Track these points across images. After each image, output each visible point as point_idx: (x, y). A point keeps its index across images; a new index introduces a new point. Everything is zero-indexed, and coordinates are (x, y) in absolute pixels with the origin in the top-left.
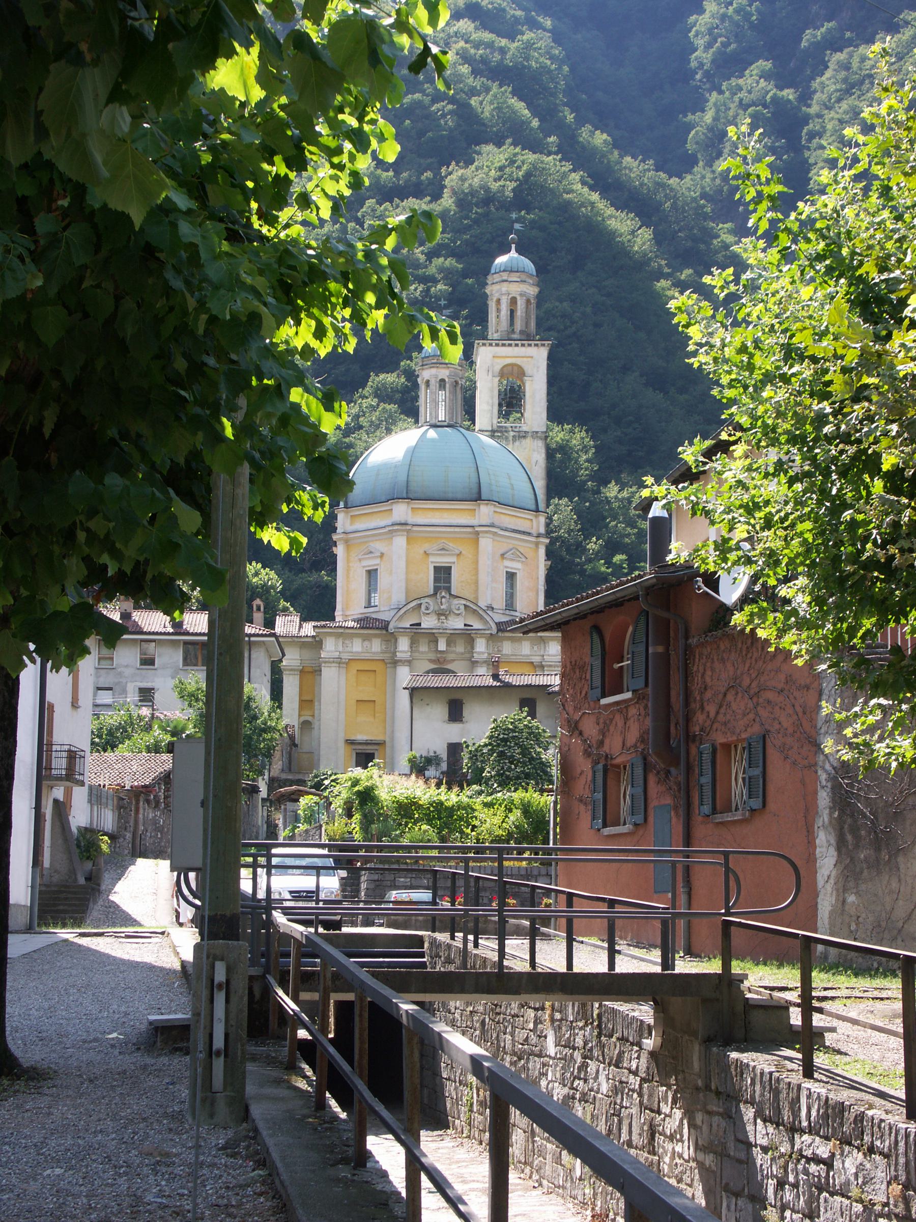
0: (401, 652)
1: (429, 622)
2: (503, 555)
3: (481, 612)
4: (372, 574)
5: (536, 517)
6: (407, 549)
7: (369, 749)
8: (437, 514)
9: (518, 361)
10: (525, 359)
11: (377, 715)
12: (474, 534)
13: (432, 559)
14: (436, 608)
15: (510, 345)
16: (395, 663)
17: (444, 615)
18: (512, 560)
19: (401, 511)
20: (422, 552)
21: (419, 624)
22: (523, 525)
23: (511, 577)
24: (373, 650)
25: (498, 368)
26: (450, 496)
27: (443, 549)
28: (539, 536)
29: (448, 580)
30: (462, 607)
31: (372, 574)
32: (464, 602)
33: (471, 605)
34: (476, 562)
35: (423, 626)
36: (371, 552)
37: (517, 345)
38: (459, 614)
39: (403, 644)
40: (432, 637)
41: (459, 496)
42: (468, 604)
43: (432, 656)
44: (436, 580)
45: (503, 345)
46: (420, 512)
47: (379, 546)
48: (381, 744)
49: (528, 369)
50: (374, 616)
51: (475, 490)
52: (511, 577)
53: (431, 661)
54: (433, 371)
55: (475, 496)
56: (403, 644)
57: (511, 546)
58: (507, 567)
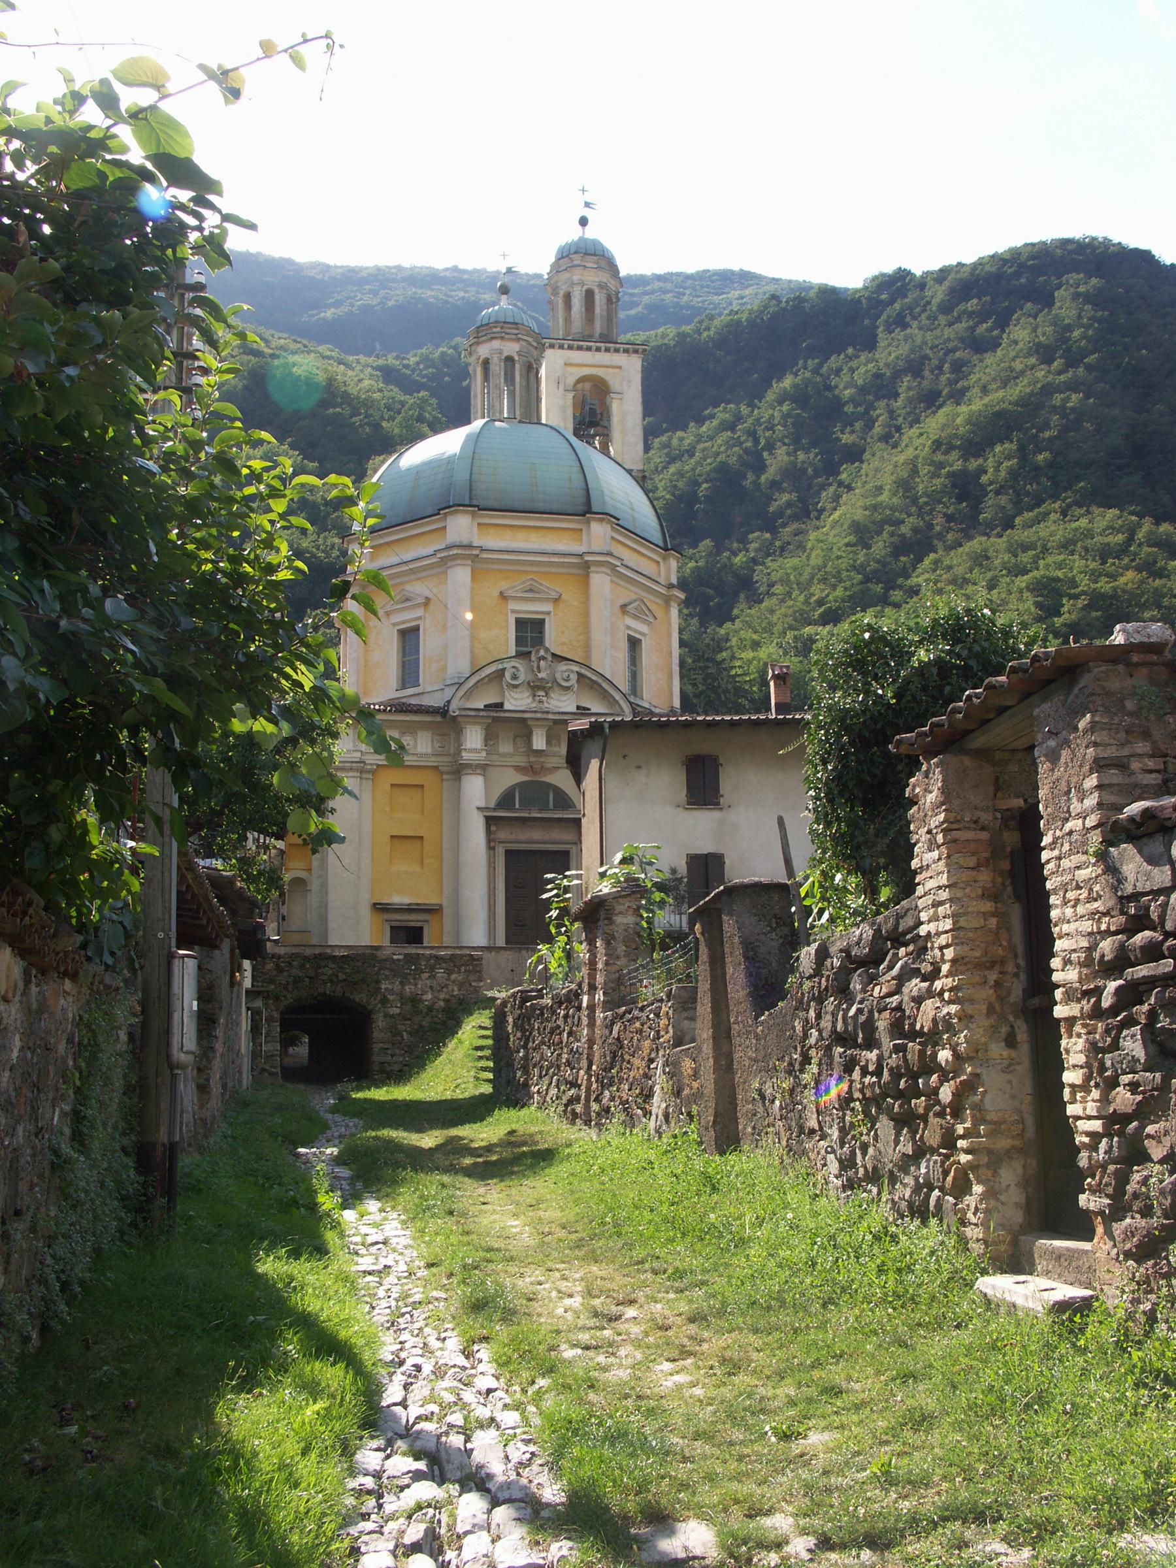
0: (471, 750)
1: (517, 702)
2: (624, 607)
3: (605, 685)
4: (409, 636)
5: (664, 558)
6: (472, 589)
7: (413, 920)
8: (520, 534)
9: (601, 372)
10: (610, 370)
11: (427, 861)
12: (583, 567)
13: (513, 605)
14: (530, 677)
15: (589, 349)
16: (458, 771)
17: (542, 688)
18: (636, 617)
19: (461, 527)
20: (496, 593)
21: (501, 705)
22: (648, 567)
23: (634, 644)
24: (419, 750)
25: (571, 380)
26: (541, 506)
27: (531, 591)
28: (670, 586)
29: (539, 640)
30: (574, 677)
31: (409, 636)
32: (576, 668)
33: (589, 674)
34: (586, 613)
35: (507, 706)
36: (407, 600)
37: (598, 349)
38: (567, 688)
39: (473, 739)
40: (522, 727)
41: (555, 507)
42: (583, 671)
43: (520, 760)
44: (519, 641)
45: (580, 348)
46: (492, 531)
47: (419, 589)
48: (434, 911)
49: (614, 383)
50: (413, 701)
51: (581, 500)
52: (634, 644)
53: (518, 769)
54: (496, 344)
55: (581, 508)
56: (473, 739)
57: (634, 597)
58: (629, 628)
